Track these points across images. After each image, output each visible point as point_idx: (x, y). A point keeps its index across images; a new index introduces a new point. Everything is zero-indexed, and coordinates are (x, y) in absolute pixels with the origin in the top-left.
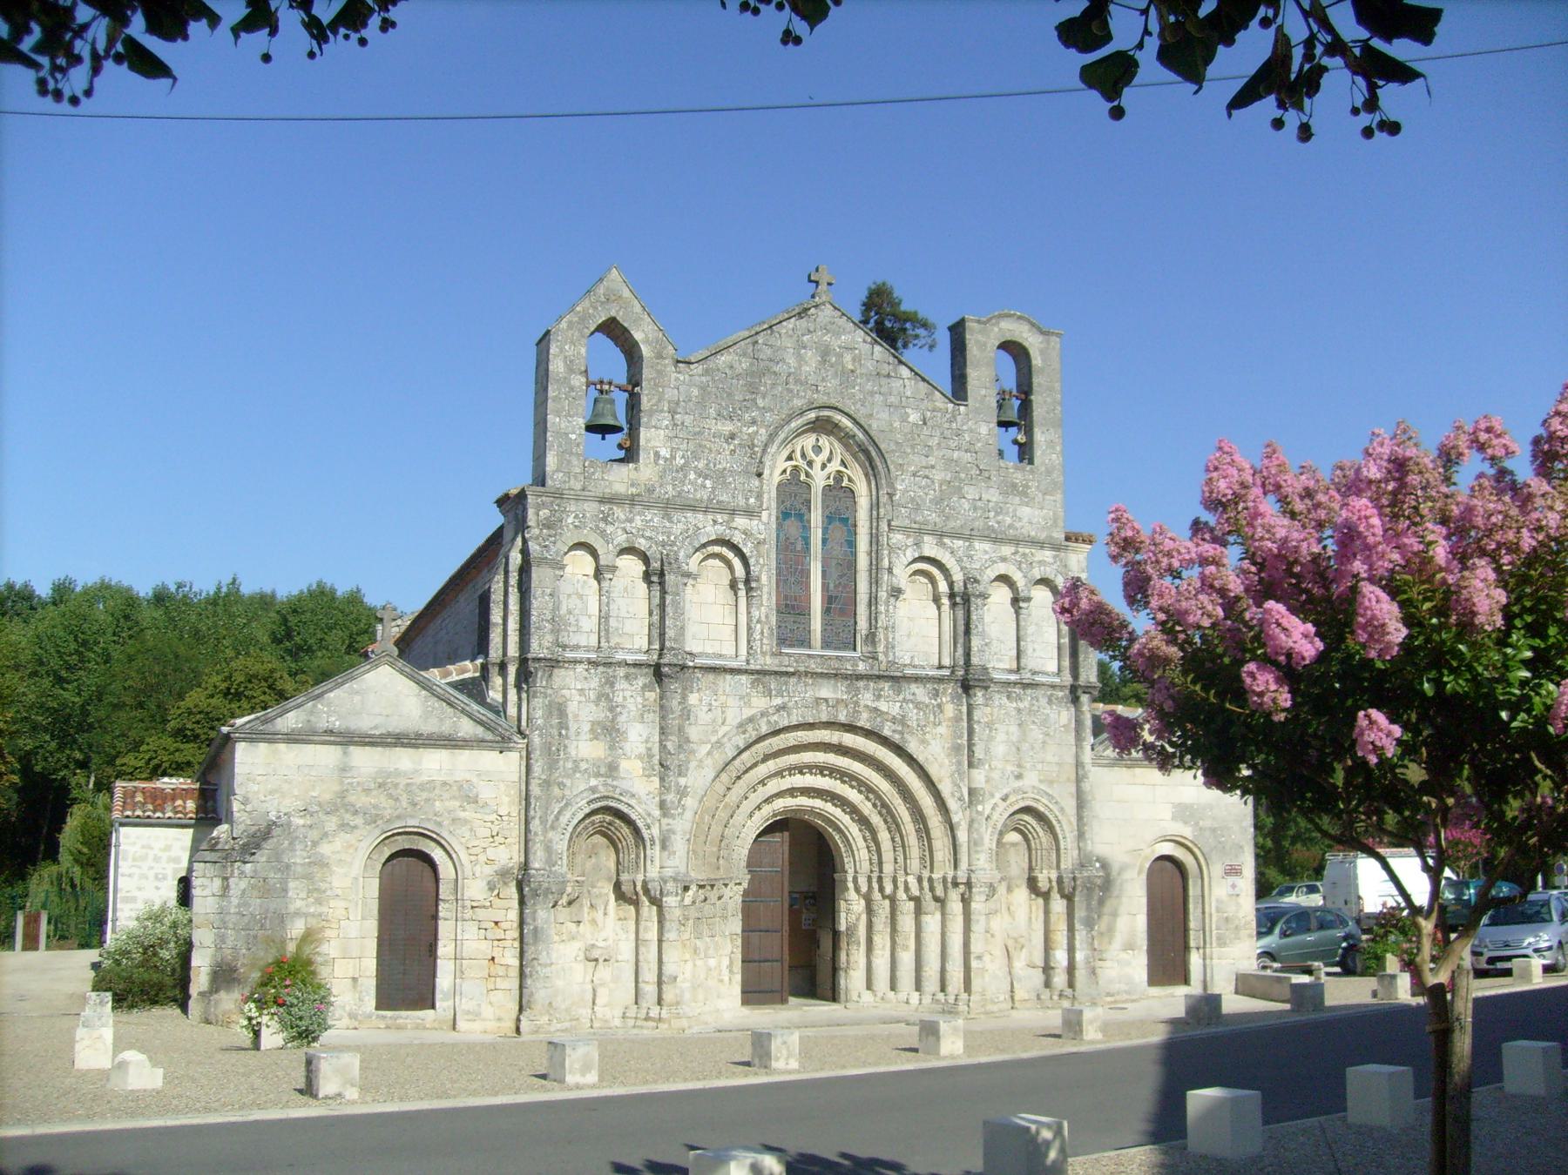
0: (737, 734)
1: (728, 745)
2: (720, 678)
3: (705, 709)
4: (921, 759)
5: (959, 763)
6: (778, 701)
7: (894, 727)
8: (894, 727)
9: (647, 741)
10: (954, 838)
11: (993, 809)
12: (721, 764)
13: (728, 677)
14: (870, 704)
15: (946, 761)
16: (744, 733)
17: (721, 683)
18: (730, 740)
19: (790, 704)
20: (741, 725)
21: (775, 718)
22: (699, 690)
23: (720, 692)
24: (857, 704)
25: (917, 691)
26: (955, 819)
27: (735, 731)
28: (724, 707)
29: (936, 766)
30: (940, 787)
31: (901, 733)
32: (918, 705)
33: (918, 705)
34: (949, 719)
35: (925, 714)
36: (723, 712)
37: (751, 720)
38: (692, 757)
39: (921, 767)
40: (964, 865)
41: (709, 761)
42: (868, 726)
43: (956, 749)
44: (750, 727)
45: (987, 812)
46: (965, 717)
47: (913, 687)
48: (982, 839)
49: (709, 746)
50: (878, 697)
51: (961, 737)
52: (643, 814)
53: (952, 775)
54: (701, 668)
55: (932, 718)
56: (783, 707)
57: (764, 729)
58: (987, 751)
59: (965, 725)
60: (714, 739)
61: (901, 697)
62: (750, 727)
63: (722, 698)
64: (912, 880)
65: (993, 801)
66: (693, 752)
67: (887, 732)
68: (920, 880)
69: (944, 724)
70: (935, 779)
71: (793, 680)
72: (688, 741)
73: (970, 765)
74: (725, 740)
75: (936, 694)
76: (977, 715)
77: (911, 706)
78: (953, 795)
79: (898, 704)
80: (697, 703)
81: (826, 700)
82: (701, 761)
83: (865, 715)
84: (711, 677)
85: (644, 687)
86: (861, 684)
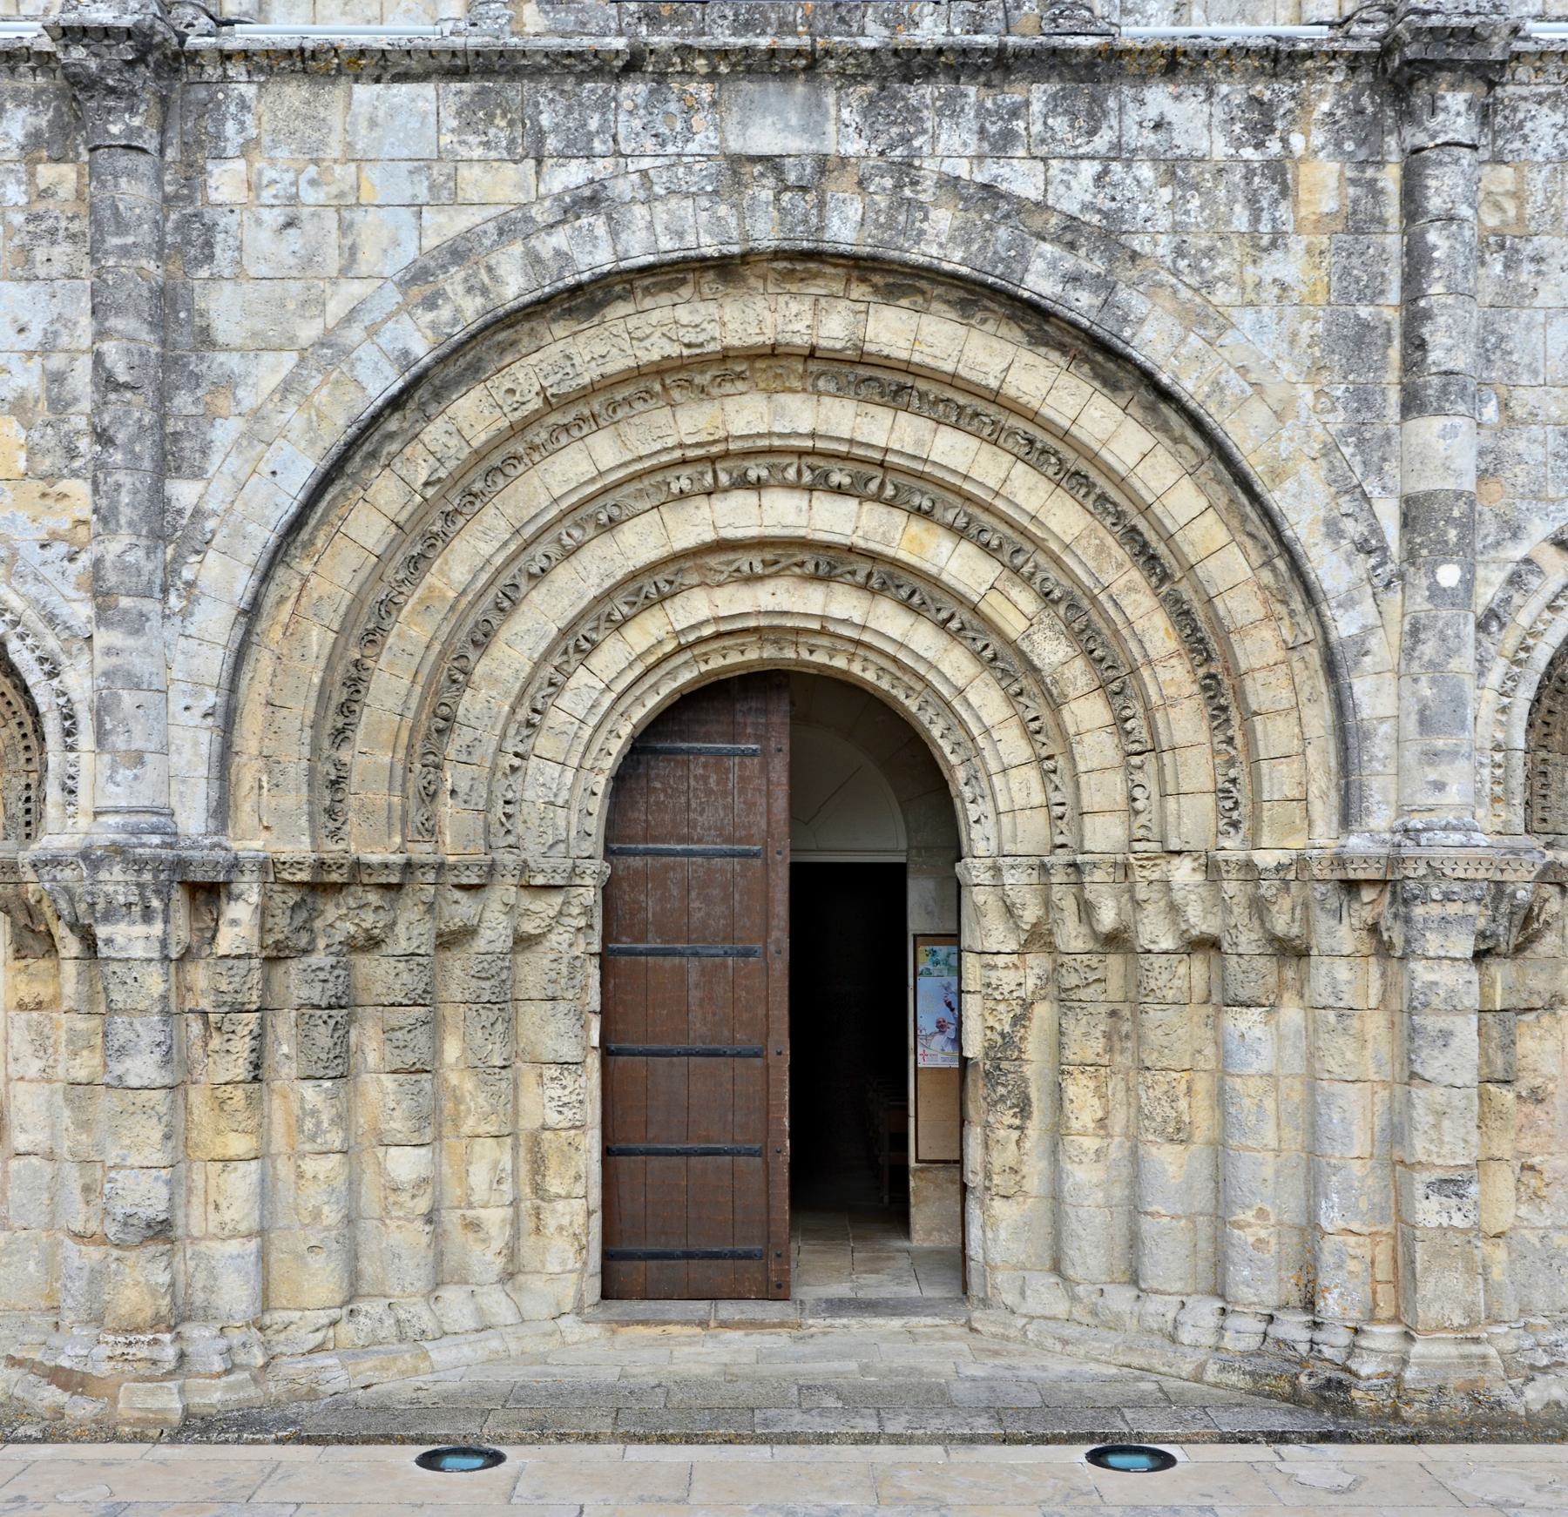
0: (404, 308)
1: (367, 352)
2: (335, 94)
3: (274, 218)
4: (1190, 386)
5: (1363, 399)
6: (571, 175)
7: (1069, 263)
8: (1069, 263)
9: (47, 348)
10: (1341, 704)
11: (1515, 580)
12: (336, 431)
13: (364, 92)
14: (962, 169)
15: (1306, 394)
16: (430, 303)
17: (336, 118)
18: (372, 331)
19: (624, 188)
20: (418, 275)
21: (560, 239)
22: (248, 148)
23: (334, 150)
24: (906, 170)
25: (1173, 111)
26: (1344, 626)
27: (393, 297)
28: (346, 206)
29: (1259, 414)
30: (1276, 498)
31: (1105, 285)
32: (1174, 169)
33: (1174, 169)
34: (1321, 223)
35: (1209, 199)
36: (345, 228)
37: (458, 252)
38: (222, 403)
39: (1196, 423)
40: (1381, 818)
41: (292, 416)
42: (954, 260)
43: (1360, 339)
44: (453, 282)
45: (1488, 592)
46: (1392, 210)
47: (1159, 98)
48: (1458, 702)
49: (289, 360)
50: (1001, 144)
51: (1373, 294)
52: (31, 617)
53: (1329, 450)
54: (246, 55)
55: (1241, 219)
56: (591, 200)
57: (514, 287)
58: (1490, 346)
59: (1394, 242)
60: (309, 331)
61: (1101, 142)
62: (453, 282)
63: (344, 174)
64: (1183, 873)
65: (1516, 552)
66: (229, 383)
67: (1039, 282)
68: (1211, 869)
69: (1298, 244)
70: (1254, 464)
71: (634, 91)
72: (205, 339)
73: (1412, 404)
74: (355, 333)
75: (1261, 120)
76: (1441, 189)
77: (1146, 171)
78: (1333, 531)
79: (1089, 169)
80: (241, 196)
81: (772, 162)
82: (257, 415)
83: (943, 219)
84: (294, 93)
85: (35, 139)
86: (925, 93)
